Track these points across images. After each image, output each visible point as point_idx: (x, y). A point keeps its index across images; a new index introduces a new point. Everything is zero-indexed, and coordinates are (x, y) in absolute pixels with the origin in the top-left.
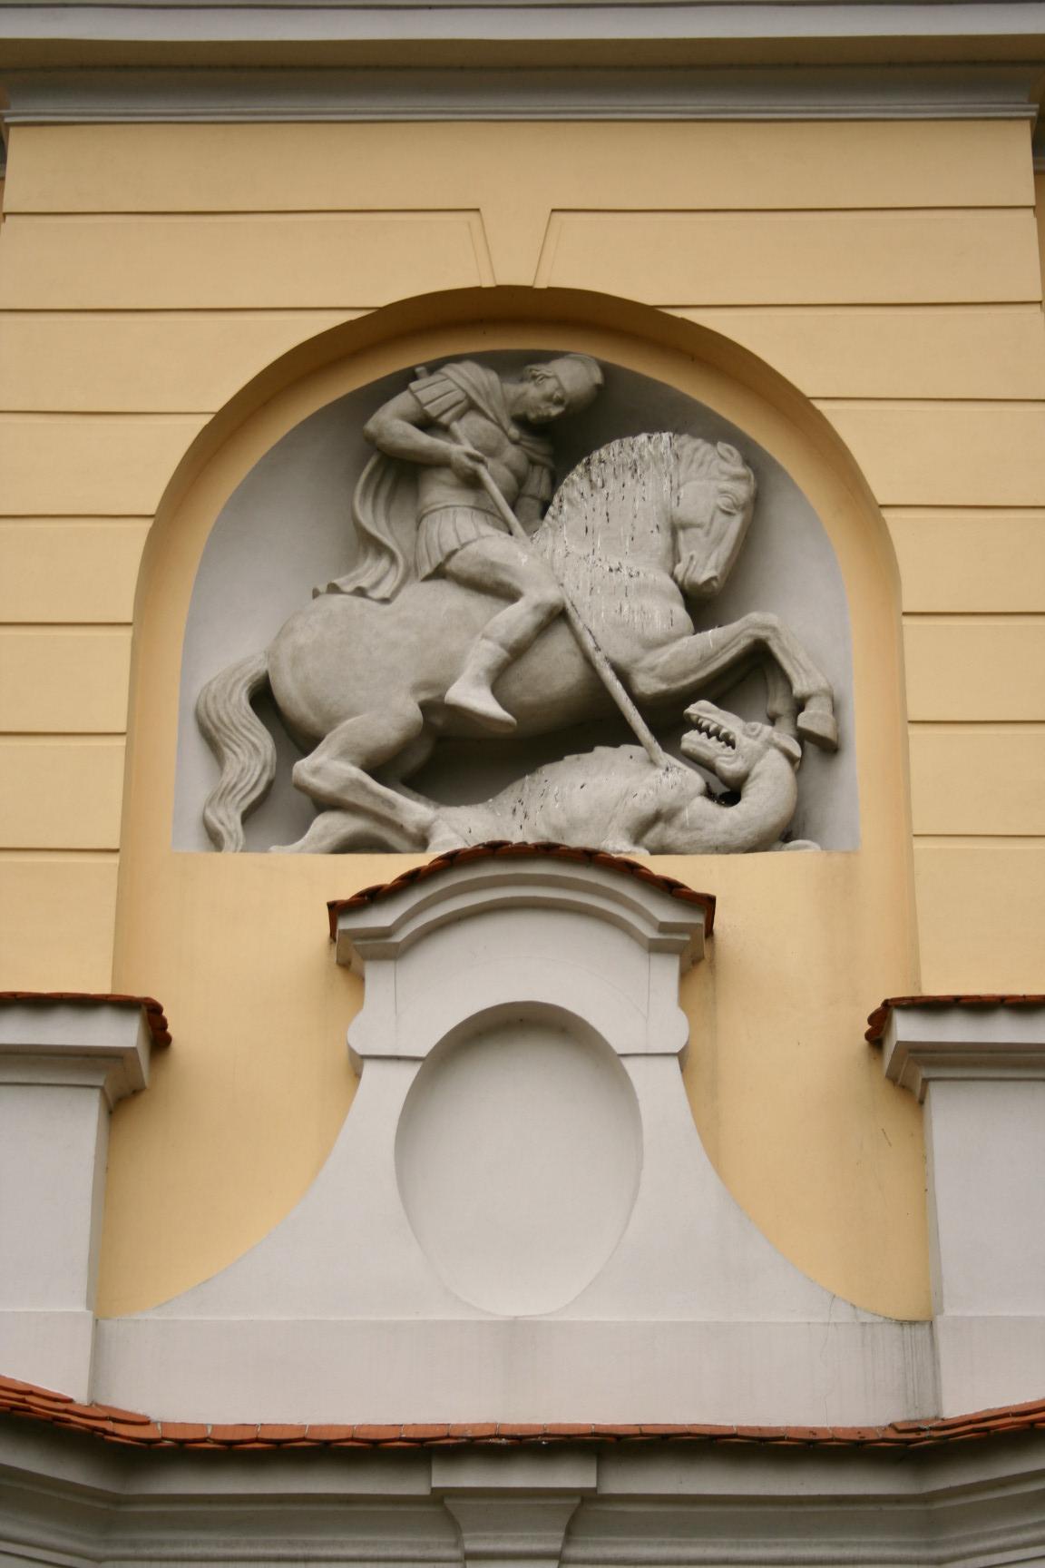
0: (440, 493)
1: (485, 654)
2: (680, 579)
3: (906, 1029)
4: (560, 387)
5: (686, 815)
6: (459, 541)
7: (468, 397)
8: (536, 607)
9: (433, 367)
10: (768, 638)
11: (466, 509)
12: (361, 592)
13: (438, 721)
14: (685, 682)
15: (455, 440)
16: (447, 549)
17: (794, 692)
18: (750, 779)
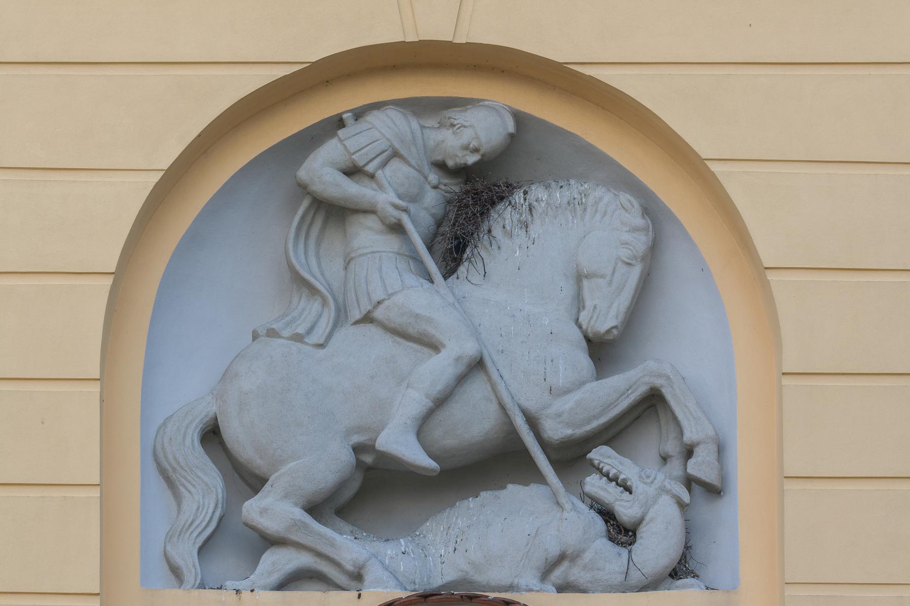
2: (584, 327)
4: (478, 138)
5: (587, 556)
6: (386, 290)
7: (392, 146)
8: (458, 359)
9: (359, 114)
10: (662, 386)
11: (391, 255)
12: (298, 338)
13: (368, 459)
14: (588, 428)
15: (381, 187)
16: (376, 297)
17: (685, 439)
18: (644, 523)
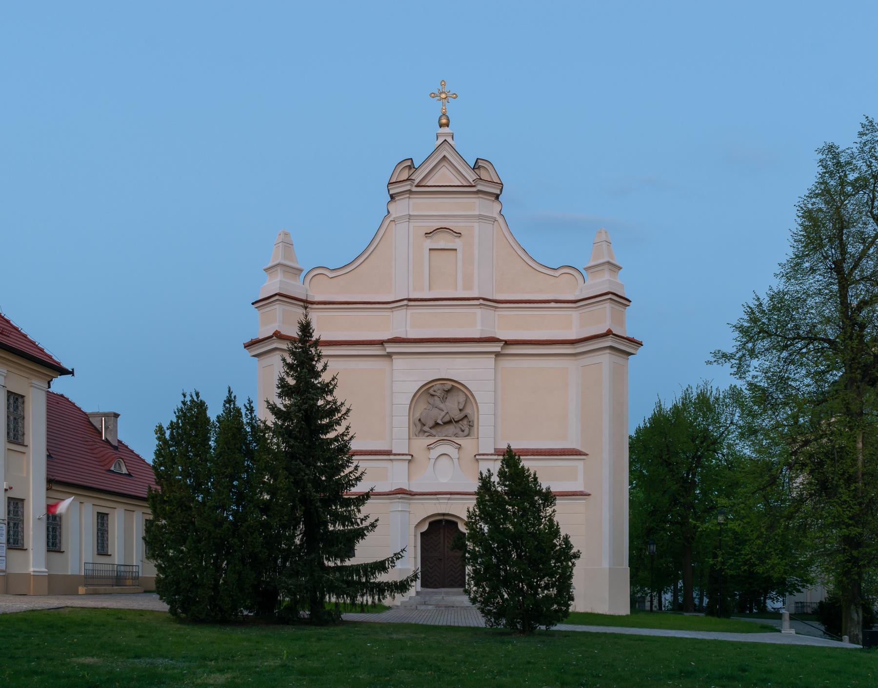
0: (436, 398)
1: (441, 417)
3: (477, 457)
